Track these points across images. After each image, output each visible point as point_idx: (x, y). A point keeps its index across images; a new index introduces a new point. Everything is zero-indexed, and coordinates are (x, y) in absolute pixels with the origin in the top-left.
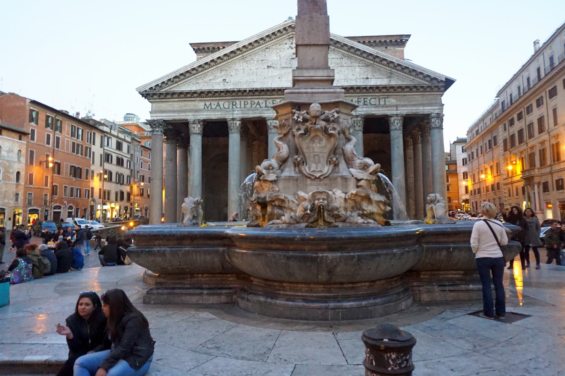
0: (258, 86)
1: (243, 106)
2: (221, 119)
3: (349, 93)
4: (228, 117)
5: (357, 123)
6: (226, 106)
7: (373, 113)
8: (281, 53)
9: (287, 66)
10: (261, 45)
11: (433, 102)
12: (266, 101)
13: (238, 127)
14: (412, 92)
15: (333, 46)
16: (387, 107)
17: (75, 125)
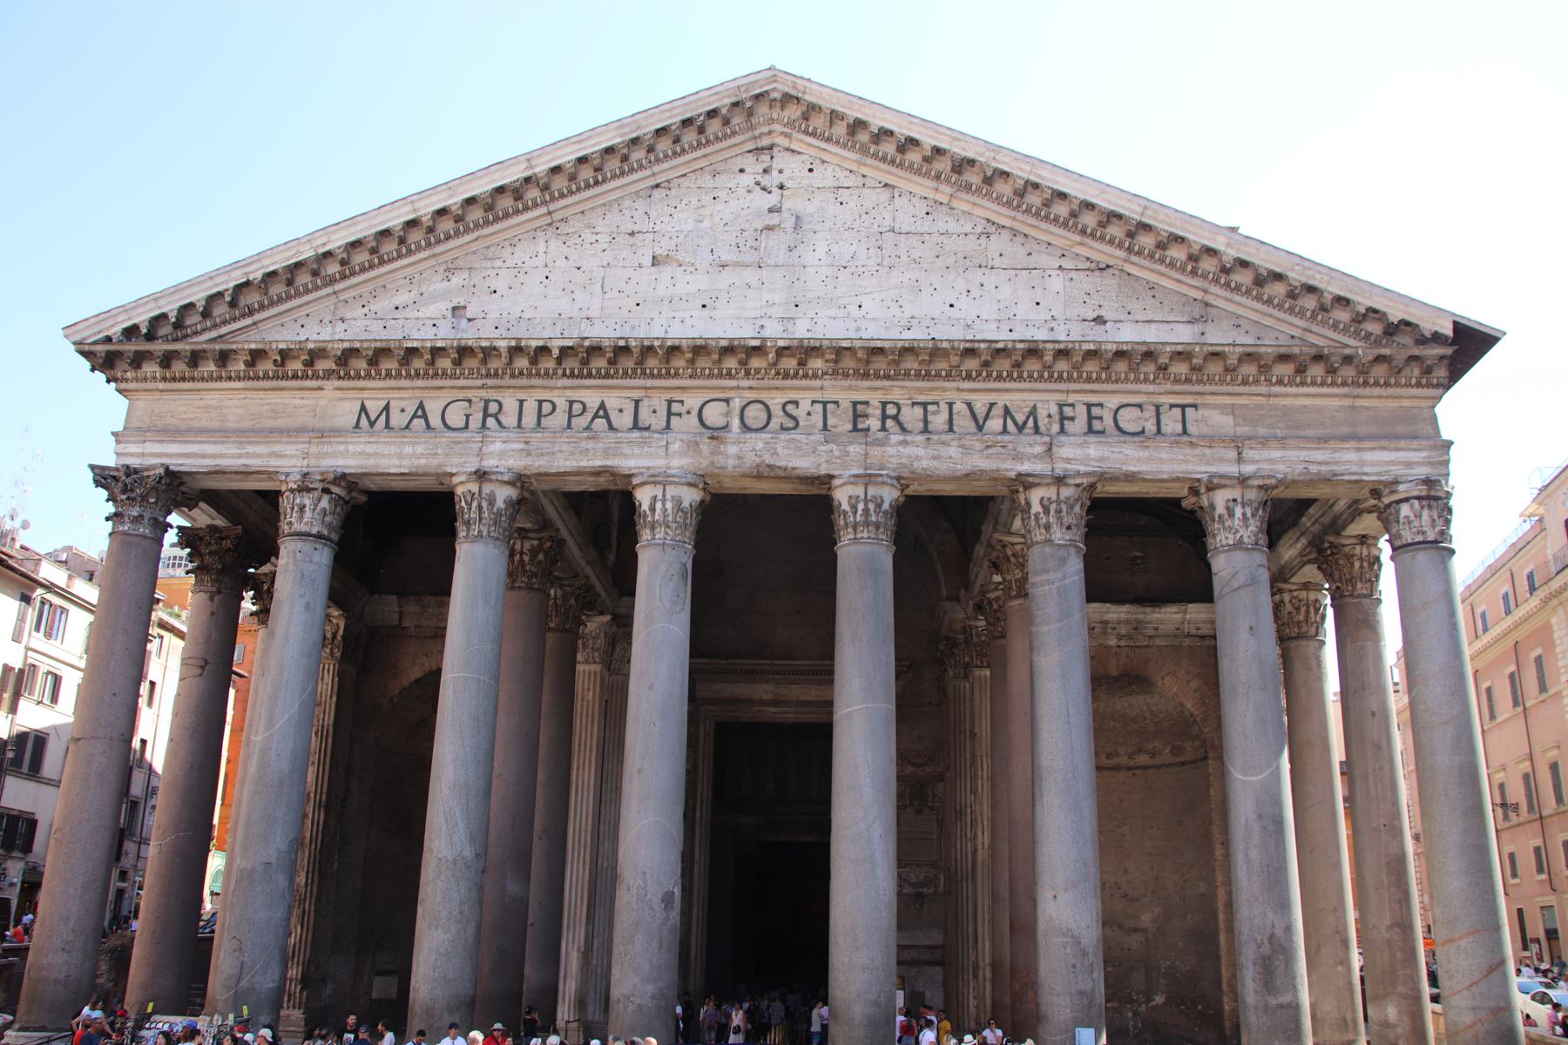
0: (604, 331)
1: (530, 419)
2: (425, 475)
3: (1020, 378)
5: (1059, 511)
6: (455, 418)
7: (1131, 468)
8: (719, 206)
9: (740, 259)
10: (632, 170)
11: (1401, 429)
12: (637, 402)
13: (499, 511)
14: (1303, 384)
15: (948, 181)
16: (1191, 444)
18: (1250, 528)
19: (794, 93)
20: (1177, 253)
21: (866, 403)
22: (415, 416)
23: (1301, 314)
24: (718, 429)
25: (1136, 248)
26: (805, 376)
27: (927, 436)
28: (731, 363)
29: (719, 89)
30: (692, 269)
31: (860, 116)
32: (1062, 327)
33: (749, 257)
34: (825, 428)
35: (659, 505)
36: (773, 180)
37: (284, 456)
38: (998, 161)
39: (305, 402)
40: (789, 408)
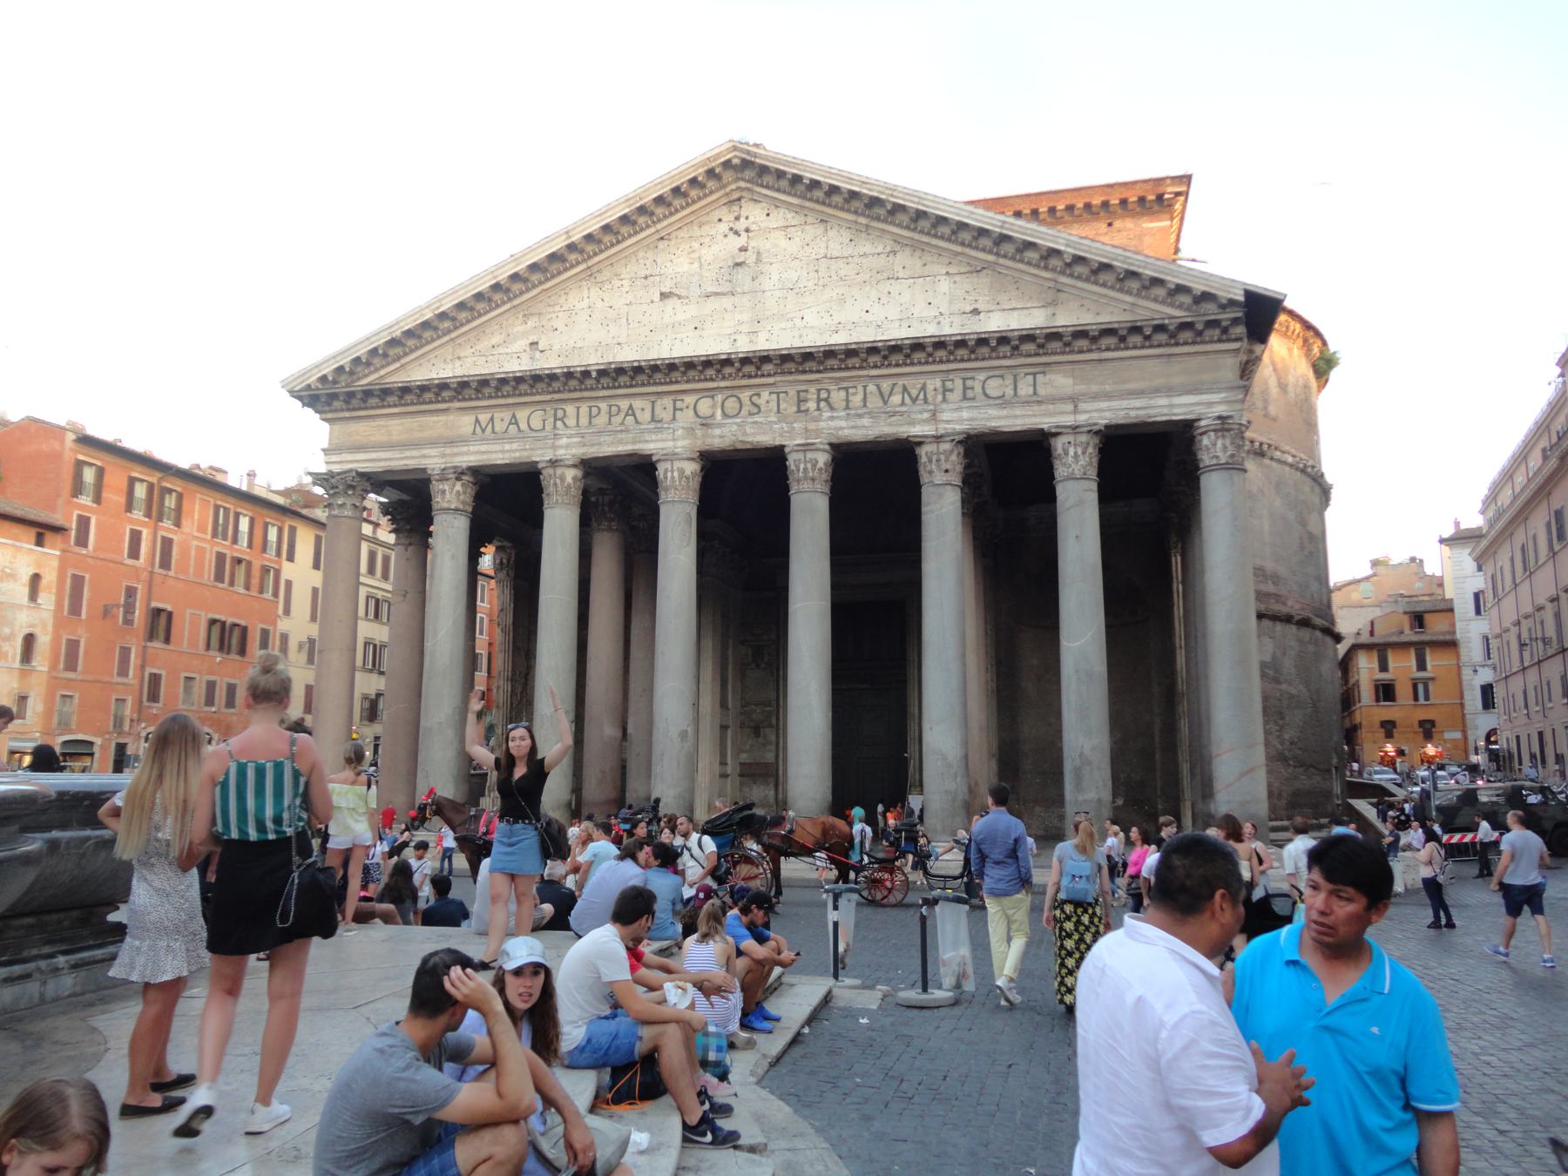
0: (628, 355)
1: (584, 421)
2: (521, 464)
3: (912, 364)
4: (540, 455)
5: (938, 461)
6: (536, 424)
7: (994, 424)
8: (703, 252)
9: (719, 290)
10: (642, 230)
12: (653, 403)
13: (569, 485)
14: (1127, 348)
15: (863, 215)
17: (230, 504)
18: (1082, 462)
19: (748, 158)
20: (1032, 255)
21: (807, 391)
22: (510, 423)
23: (1129, 292)
24: (704, 418)
25: (1002, 252)
26: (763, 376)
27: (847, 411)
28: (710, 372)
29: (693, 163)
30: (687, 301)
31: (795, 171)
32: (946, 321)
33: (726, 288)
34: (778, 411)
35: (669, 474)
36: (741, 225)
37: (430, 457)
38: (895, 197)
39: (440, 418)
40: (754, 398)
